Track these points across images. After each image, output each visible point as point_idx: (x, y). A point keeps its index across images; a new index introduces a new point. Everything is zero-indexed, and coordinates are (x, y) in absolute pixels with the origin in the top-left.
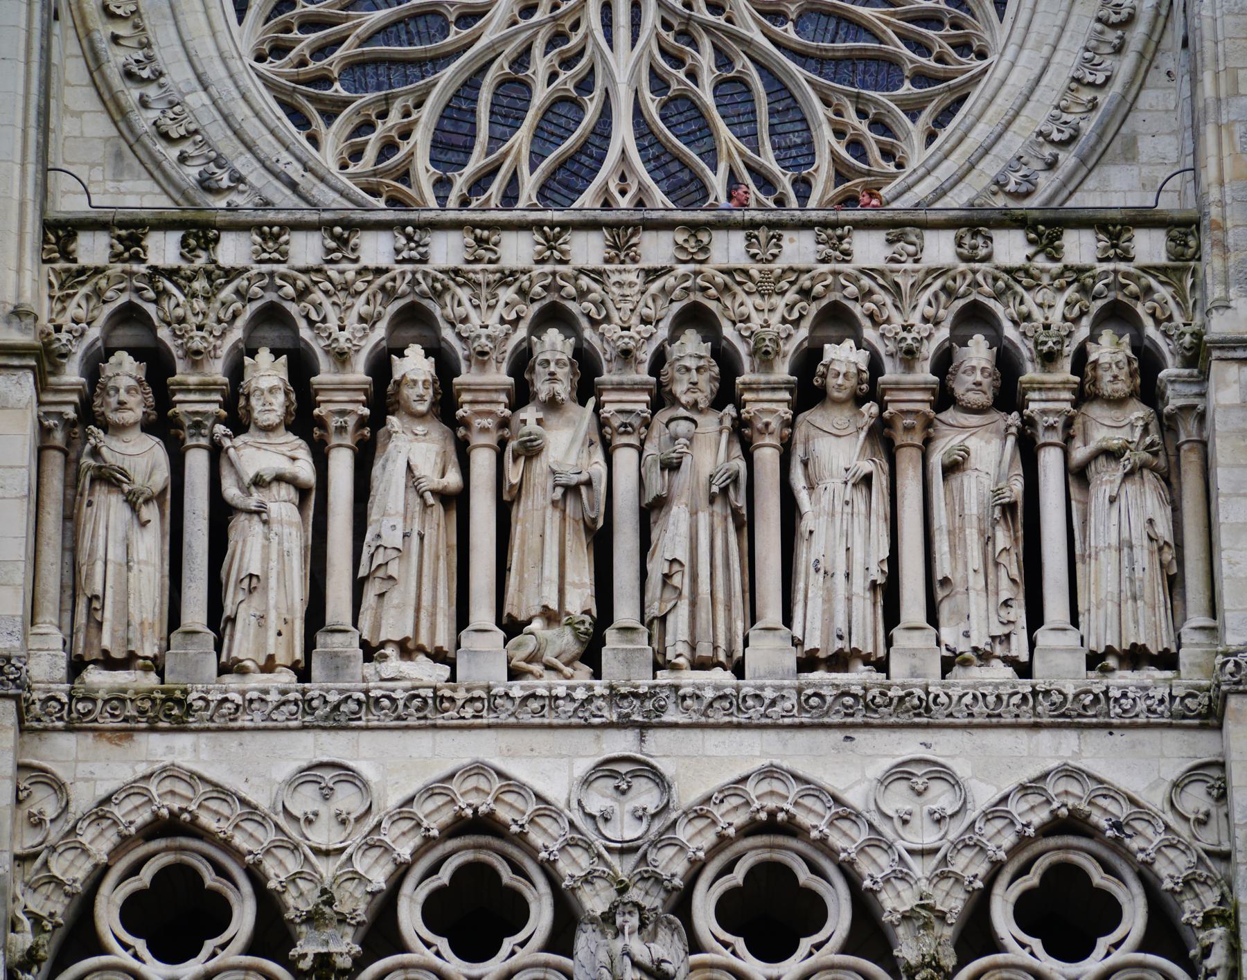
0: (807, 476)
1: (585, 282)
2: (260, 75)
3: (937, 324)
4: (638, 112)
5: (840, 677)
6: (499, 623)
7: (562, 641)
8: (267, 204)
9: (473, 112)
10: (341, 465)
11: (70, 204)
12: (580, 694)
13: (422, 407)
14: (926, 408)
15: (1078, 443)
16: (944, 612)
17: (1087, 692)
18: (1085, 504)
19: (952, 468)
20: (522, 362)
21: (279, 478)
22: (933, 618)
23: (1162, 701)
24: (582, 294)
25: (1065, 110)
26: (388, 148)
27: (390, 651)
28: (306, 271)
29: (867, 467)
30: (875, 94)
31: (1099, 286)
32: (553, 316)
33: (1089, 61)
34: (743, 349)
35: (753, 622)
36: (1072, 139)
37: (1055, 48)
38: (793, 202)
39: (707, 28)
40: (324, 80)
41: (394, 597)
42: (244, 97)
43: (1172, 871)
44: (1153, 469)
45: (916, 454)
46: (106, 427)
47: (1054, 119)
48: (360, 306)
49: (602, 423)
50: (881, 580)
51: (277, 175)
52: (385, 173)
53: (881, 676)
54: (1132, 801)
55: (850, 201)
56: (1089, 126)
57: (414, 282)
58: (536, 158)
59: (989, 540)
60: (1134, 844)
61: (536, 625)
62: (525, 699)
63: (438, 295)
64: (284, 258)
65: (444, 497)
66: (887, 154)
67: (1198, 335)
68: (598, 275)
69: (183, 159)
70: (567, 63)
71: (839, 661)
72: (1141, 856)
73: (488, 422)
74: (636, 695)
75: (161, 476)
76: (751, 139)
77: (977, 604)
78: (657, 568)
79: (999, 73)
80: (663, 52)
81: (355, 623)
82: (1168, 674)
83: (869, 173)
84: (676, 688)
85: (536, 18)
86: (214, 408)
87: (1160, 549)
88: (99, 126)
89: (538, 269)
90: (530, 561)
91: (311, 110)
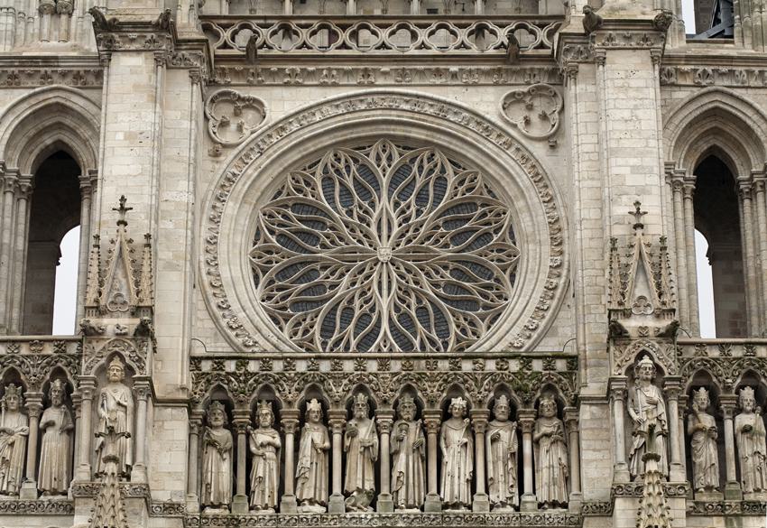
0: (446, 444)
1: (371, 377)
2: (263, 306)
3: (490, 392)
4: (390, 319)
5: (457, 511)
6: (342, 493)
7: (365, 499)
8: (265, 351)
9: (335, 319)
10: (290, 440)
11: (199, 352)
12: (369, 517)
13: (317, 420)
14: (486, 420)
15: (536, 432)
16: (491, 491)
18: (538, 452)
19: (494, 440)
20: (350, 405)
21: (269, 444)
22: (487, 491)
24: (371, 382)
25: (533, 318)
26: (306, 331)
27: (306, 502)
28: (278, 374)
29: (465, 440)
30: (470, 313)
31: (544, 379)
32: (361, 389)
34: (424, 400)
35: (427, 492)
36: (536, 328)
38: (442, 350)
39: (413, 290)
40: (284, 308)
41: (307, 485)
42: (257, 314)
44: (561, 441)
45: (482, 436)
46: (211, 427)
47: (529, 321)
48: (296, 385)
49: (377, 425)
50: (470, 478)
51: (268, 341)
52: (304, 340)
53: (469, 511)
55: (461, 349)
56: (543, 324)
57: (314, 377)
58: (356, 335)
59: (505, 465)
61: (355, 494)
62: (351, 519)
63: (322, 382)
64: (271, 369)
65: (324, 450)
66: (474, 333)
67: (576, 396)
68: (376, 375)
69: (237, 335)
70: (366, 302)
71: (456, 506)
73: (337, 425)
74: (388, 517)
75: (230, 444)
76: (428, 327)
77: (501, 487)
78: (395, 475)
79: (512, 306)
80: (399, 298)
81: (295, 493)
83: (467, 340)
84: (401, 515)
85: (356, 286)
86: (248, 420)
88: (209, 324)
89: (356, 373)
90: (353, 472)
91: (280, 318)
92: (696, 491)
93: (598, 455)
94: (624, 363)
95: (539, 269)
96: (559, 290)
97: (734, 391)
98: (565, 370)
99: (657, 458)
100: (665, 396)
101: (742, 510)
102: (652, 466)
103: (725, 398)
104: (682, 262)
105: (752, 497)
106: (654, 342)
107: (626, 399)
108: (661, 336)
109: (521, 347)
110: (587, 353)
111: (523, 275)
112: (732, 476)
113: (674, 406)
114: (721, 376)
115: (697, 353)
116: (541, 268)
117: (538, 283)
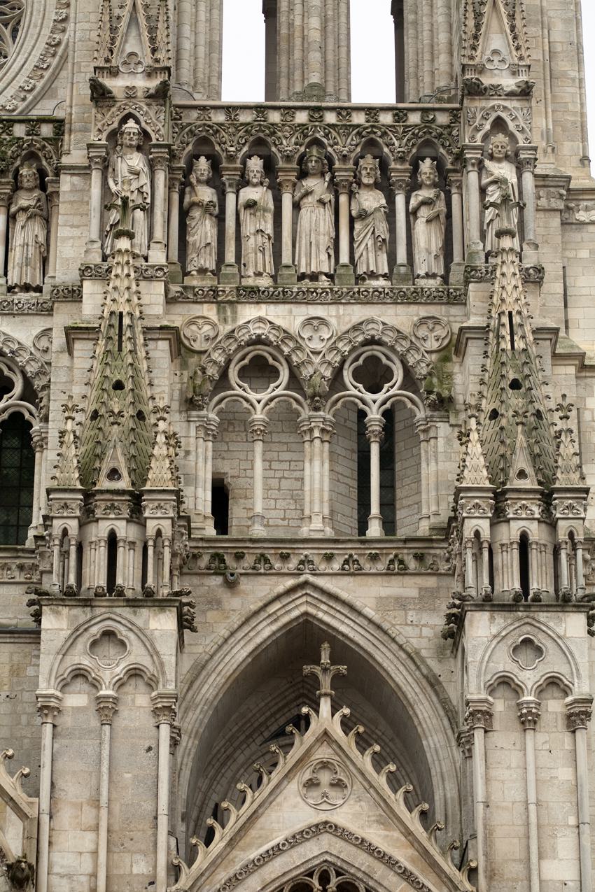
17: (5, 301)
23: (34, 305)
33: (42, 59)
36: (32, 90)
37: (30, 55)
43: (32, 370)
47: (26, 81)
54: (19, 343)
56: (40, 85)
60: (18, 359)
72: (20, 364)
79: (9, 64)
82: (38, 294)
87: (40, 247)
92: (186, 274)
93: (76, 232)
94: (106, 127)
95: (42, 23)
96: (62, 47)
97: (239, 161)
98: (51, 135)
99: (131, 236)
100: (152, 165)
101: (237, 296)
102: (123, 244)
103: (227, 169)
104: (203, 16)
105: (250, 282)
106: (143, 105)
107: (106, 168)
108: (150, 97)
109: (14, 110)
110: (73, 117)
111: (25, 29)
112: (230, 257)
113: (161, 177)
114: (225, 143)
115: (198, 118)
116: (45, 22)
117: (39, 40)
